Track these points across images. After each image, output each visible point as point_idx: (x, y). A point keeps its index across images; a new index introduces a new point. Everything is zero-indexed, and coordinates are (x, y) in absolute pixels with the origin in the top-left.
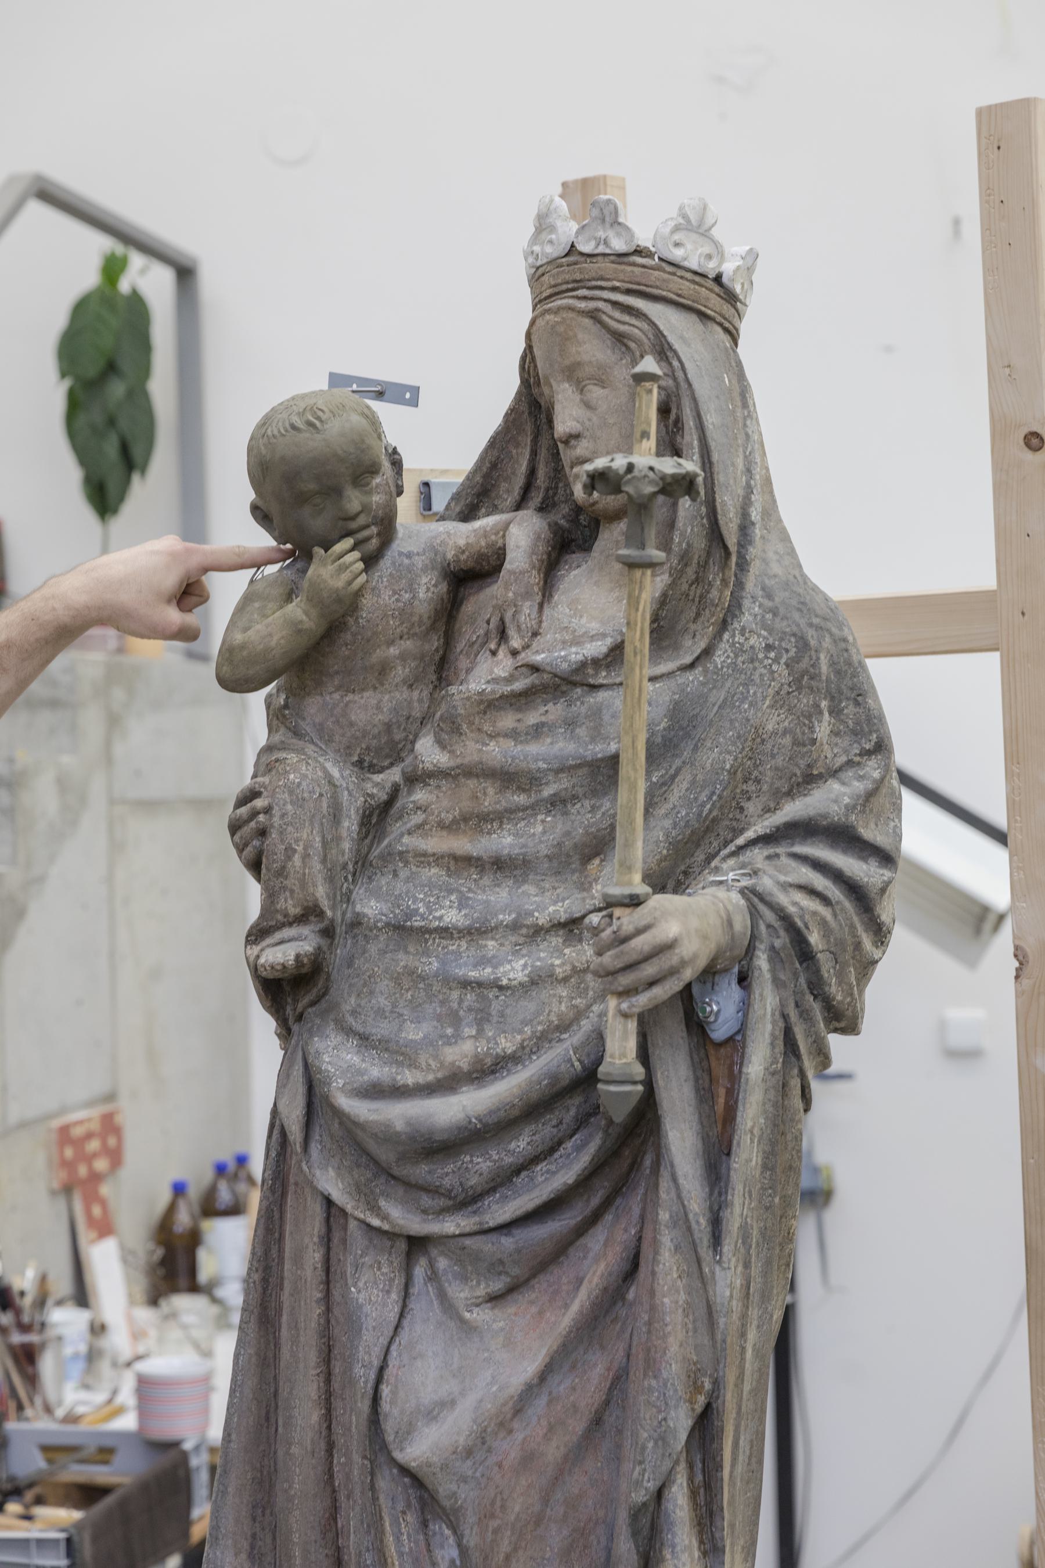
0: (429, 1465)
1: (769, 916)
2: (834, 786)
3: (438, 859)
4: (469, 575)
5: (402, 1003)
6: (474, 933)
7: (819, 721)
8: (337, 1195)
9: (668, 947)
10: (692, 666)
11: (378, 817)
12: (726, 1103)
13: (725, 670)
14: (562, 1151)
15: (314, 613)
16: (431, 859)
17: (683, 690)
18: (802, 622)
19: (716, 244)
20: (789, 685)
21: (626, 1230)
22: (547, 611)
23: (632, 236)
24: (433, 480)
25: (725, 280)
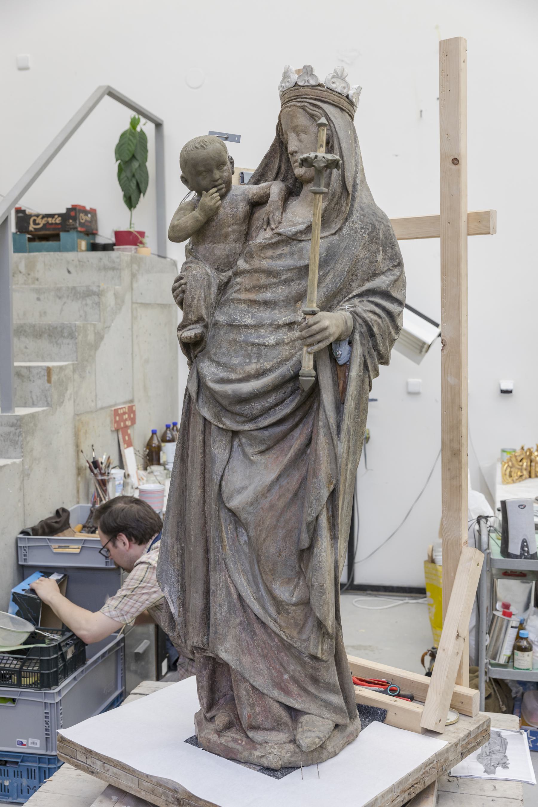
0: (238, 508)
1: (360, 321)
2: (383, 278)
3: (244, 301)
4: (257, 204)
6: (257, 327)
7: (379, 254)
8: (208, 417)
9: (325, 329)
10: (335, 234)
11: (224, 287)
12: (343, 386)
14: (286, 402)
15: (202, 214)
18: (374, 219)
19: (347, 83)
21: (307, 429)
22: (284, 215)
23: (318, 79)
24: (244, 172)
25: (350, 97)
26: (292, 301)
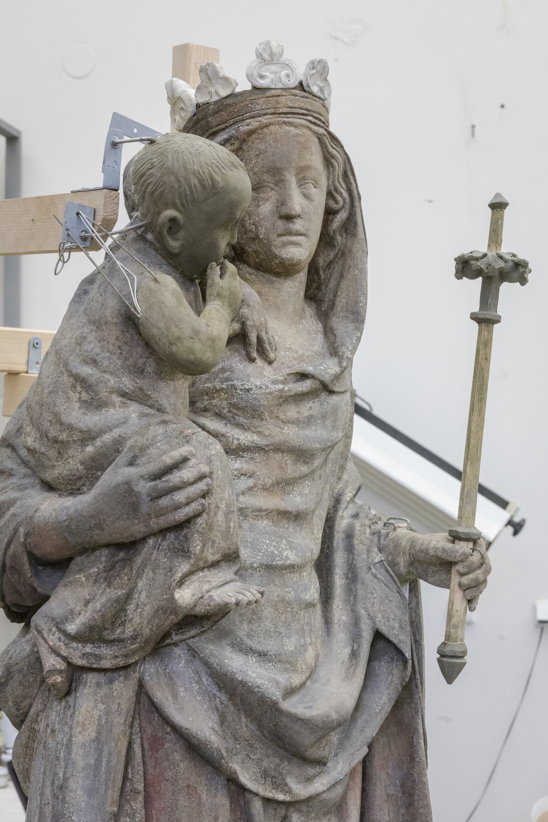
5: (280, 624)
16: (264, 514)
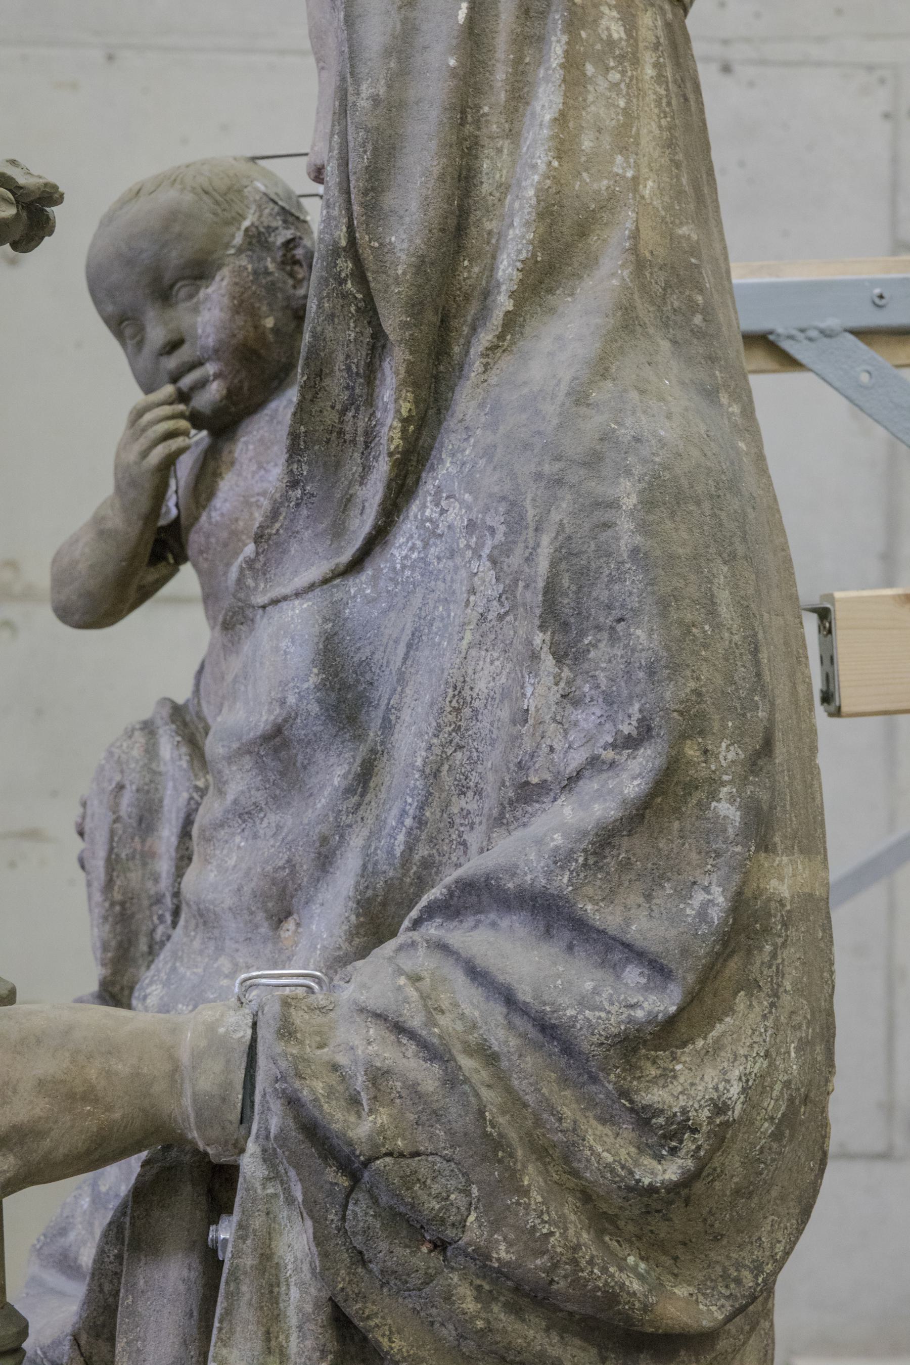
13: (407, 573)
17: (338, 614)
20: (502, 605)
26: (260, 916)
